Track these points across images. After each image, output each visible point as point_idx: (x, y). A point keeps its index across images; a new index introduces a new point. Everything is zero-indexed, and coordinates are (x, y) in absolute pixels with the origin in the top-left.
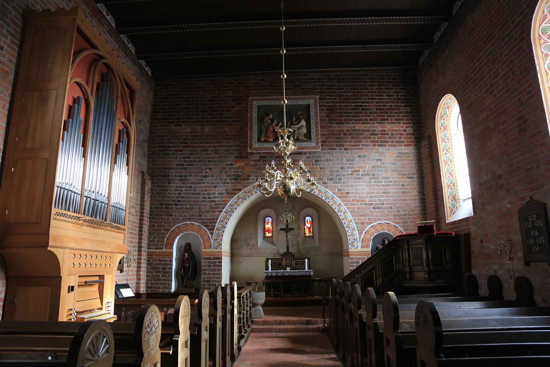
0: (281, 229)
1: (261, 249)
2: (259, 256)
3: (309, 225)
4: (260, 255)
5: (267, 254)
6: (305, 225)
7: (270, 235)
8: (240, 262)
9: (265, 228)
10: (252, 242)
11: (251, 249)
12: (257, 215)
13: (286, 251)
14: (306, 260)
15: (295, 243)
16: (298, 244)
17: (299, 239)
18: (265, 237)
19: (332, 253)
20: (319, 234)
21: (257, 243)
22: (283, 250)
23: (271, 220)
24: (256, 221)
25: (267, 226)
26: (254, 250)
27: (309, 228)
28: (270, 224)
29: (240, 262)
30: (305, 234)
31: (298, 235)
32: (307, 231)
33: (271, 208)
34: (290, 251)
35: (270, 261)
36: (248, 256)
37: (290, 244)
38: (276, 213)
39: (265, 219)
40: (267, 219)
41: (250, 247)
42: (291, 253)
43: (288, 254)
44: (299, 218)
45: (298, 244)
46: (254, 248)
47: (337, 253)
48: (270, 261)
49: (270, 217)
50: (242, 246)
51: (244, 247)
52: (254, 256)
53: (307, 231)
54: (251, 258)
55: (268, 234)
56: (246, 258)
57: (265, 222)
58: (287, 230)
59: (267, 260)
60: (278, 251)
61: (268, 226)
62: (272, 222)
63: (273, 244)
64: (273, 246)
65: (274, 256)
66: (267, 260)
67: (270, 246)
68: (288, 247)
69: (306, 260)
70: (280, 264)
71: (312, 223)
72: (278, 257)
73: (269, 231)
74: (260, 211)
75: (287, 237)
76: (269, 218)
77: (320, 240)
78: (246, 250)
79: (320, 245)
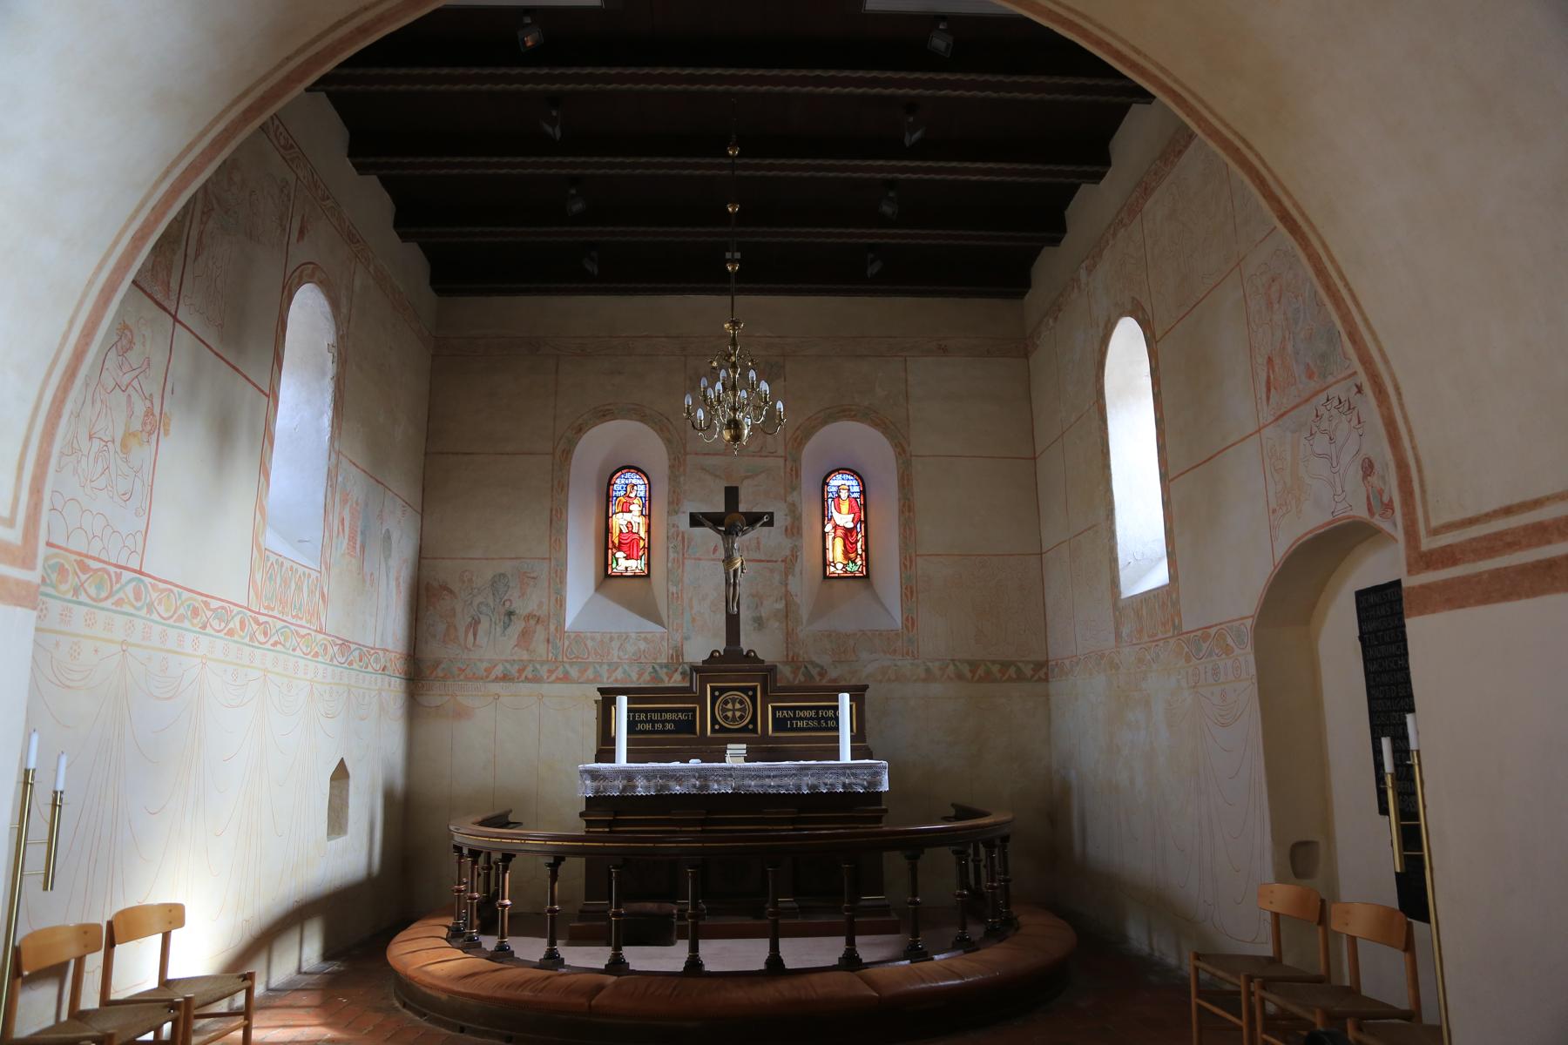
0: (696, 520)
1: (578, 637)
2: (566, 678)
3: (844, 519)
4: (574, 672)
5: (613, 667)
6: (825, 516)
7: (636, 566)
8: (461, 714)
9: (608, 530)
10: (530, 602)
11: (525, 635)
12: (568, 454)
13: (720, 645)
14: (845, 699)
15: (773, 605)
16: (788, 613)
17: (794, 585)
18: (606, 576)
19: (974, 665)
20: (907, 562)
21: (561, 603)
22: (703, 644)
23: (641, 490)
24: (559, 486)
25: (619, 521)
26: (541, 649)
27: (848, 533)
28: (635, 508)
29: (461, 714)
30: (825, 564)
31: (791, 562)
32: (836, 550)
33: (643, 418)
34: (745, 645)
35: (623, 701)
36: (505, 678)
37: (745, 616)
38: (668, 442)
39: (610, 484)
40: (619, 483)
41: (517, 627)
42: (750, 658)
43: (731, 663)
44: (796, 472)
45: (788, 613)
46: (540, 634)
47: (1005, 665)
48: (623, 701)
49: (638, 470)
50: (476, 623)
51: (484, 624)
52: (537, 679)
53: (836, 550)
54: (524, 688)
55: (624, 564)
56: (496, 688)
57: (608, 498)
58: (729, 520)
59: (607, 698)
60: (678, 653)
61: (628, 520)
62: (648, 501)
63: (648, 611)
64: (651, 626)
65: (655, 677)
66: (607, 698)
67: (632, 623)
68: (733, 622)
69: (845, 699)
70: (687, 726)
71: (862, 508)
72: (676, 681)
73: (628, 545)
74: (580, 430)
75: (729, 560)
76: (635, 479)
77: (909, 591)
78: (494, 646)
79: (910, 621)
